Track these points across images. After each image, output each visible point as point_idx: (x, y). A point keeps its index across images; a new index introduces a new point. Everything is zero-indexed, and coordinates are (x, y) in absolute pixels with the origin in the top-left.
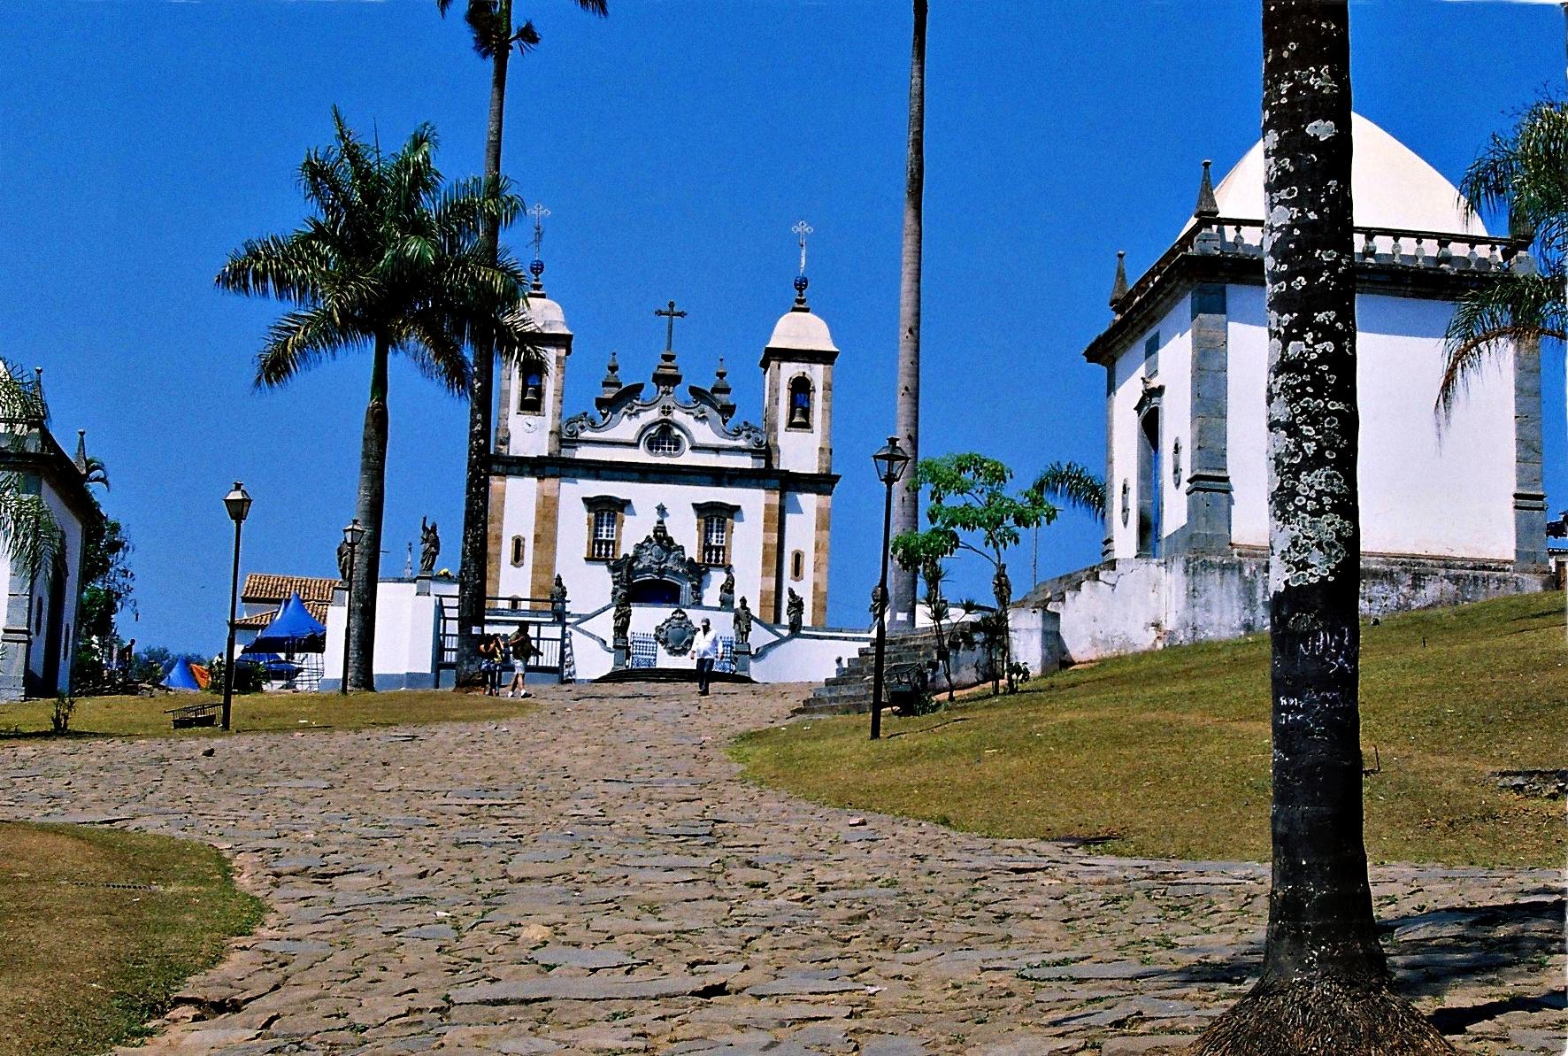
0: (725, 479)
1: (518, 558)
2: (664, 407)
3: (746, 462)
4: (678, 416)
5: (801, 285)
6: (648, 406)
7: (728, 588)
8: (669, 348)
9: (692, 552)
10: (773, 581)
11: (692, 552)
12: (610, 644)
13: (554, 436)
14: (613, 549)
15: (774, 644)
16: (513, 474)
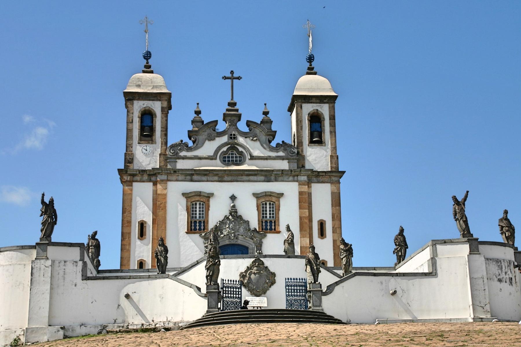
0: (273, 178)
1: (142, 234)
2: (231, 135)
3: (284, 165)
4: (241, 140)
5: (311, 59)
6: (221, 134)
7: (290, 242)
8: (232, 99)
9: (254, 224)
10: (308, 240)
11: (254, 224)
12: (204, 291)
13: (162, 156)
14: (204, 226)
15: (337, 283)
16: (137, 181)
